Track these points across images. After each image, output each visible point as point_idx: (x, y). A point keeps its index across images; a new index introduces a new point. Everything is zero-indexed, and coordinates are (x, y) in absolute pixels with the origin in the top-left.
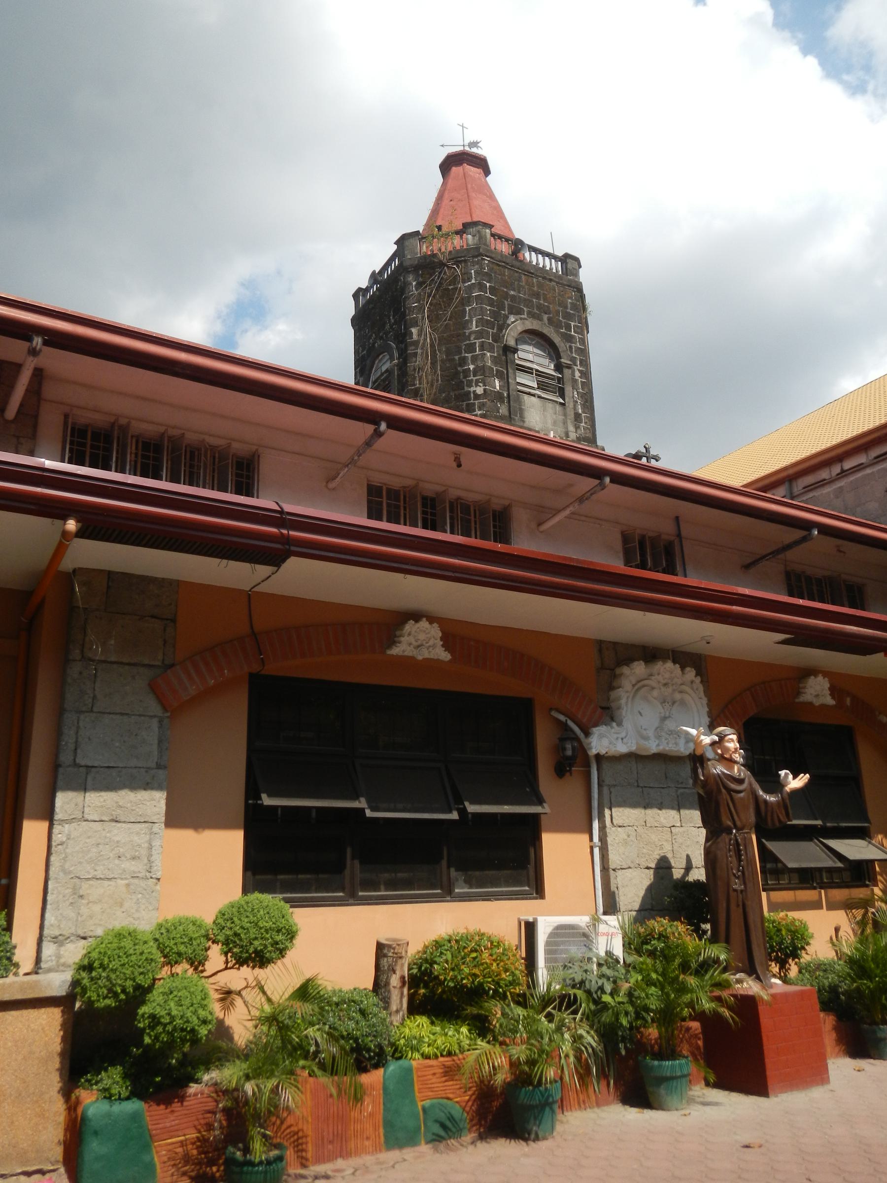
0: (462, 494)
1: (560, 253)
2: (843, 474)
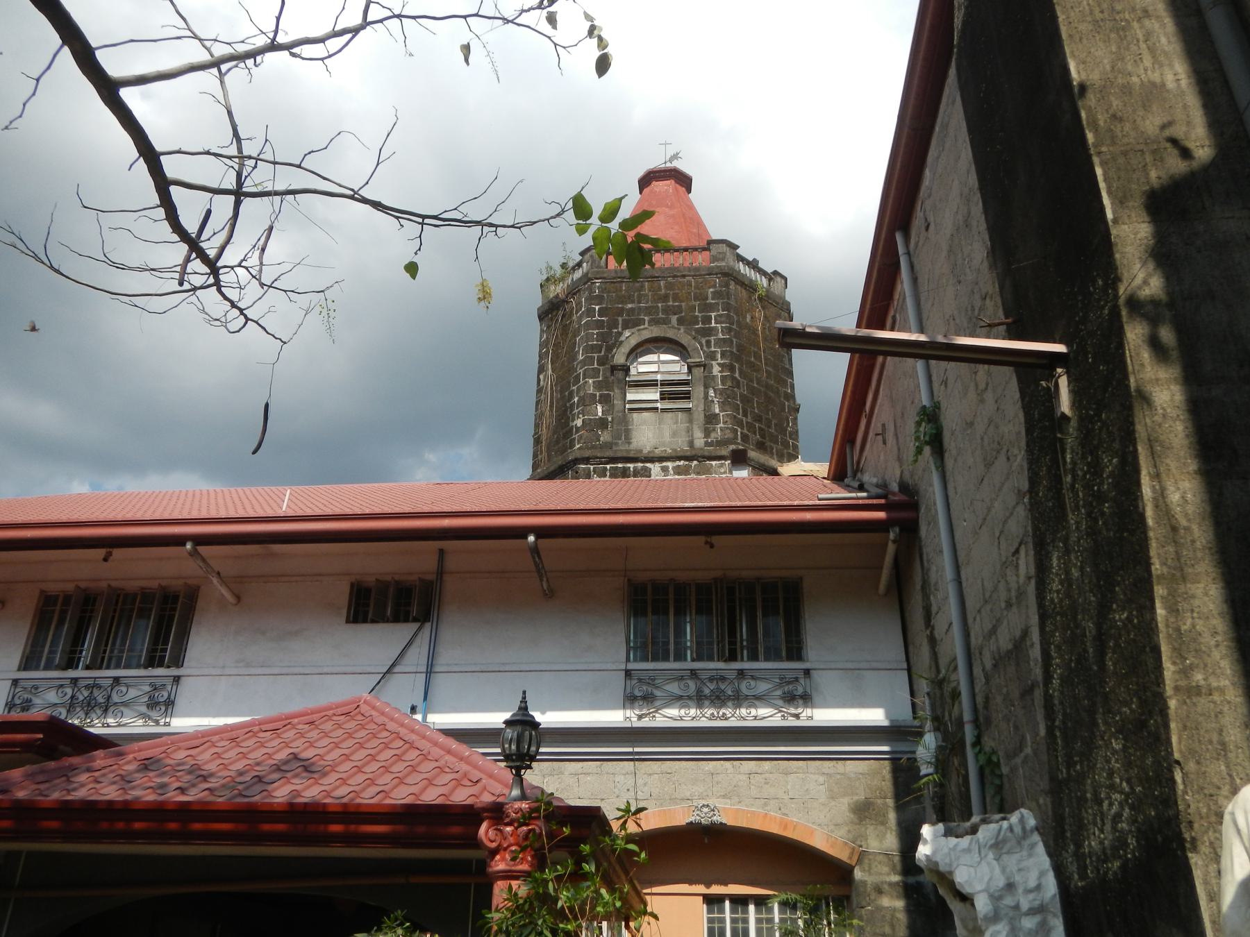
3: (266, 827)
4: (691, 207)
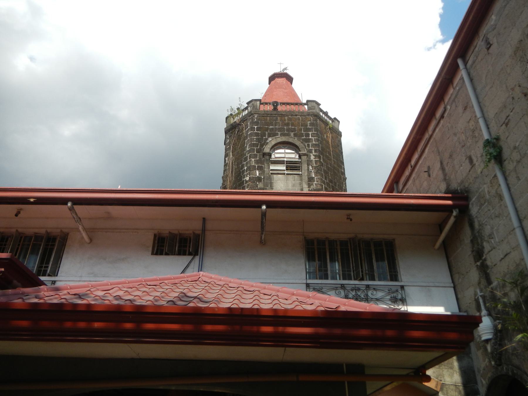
0: (36, 231)
3: (209, 328)
4: (293, 90)
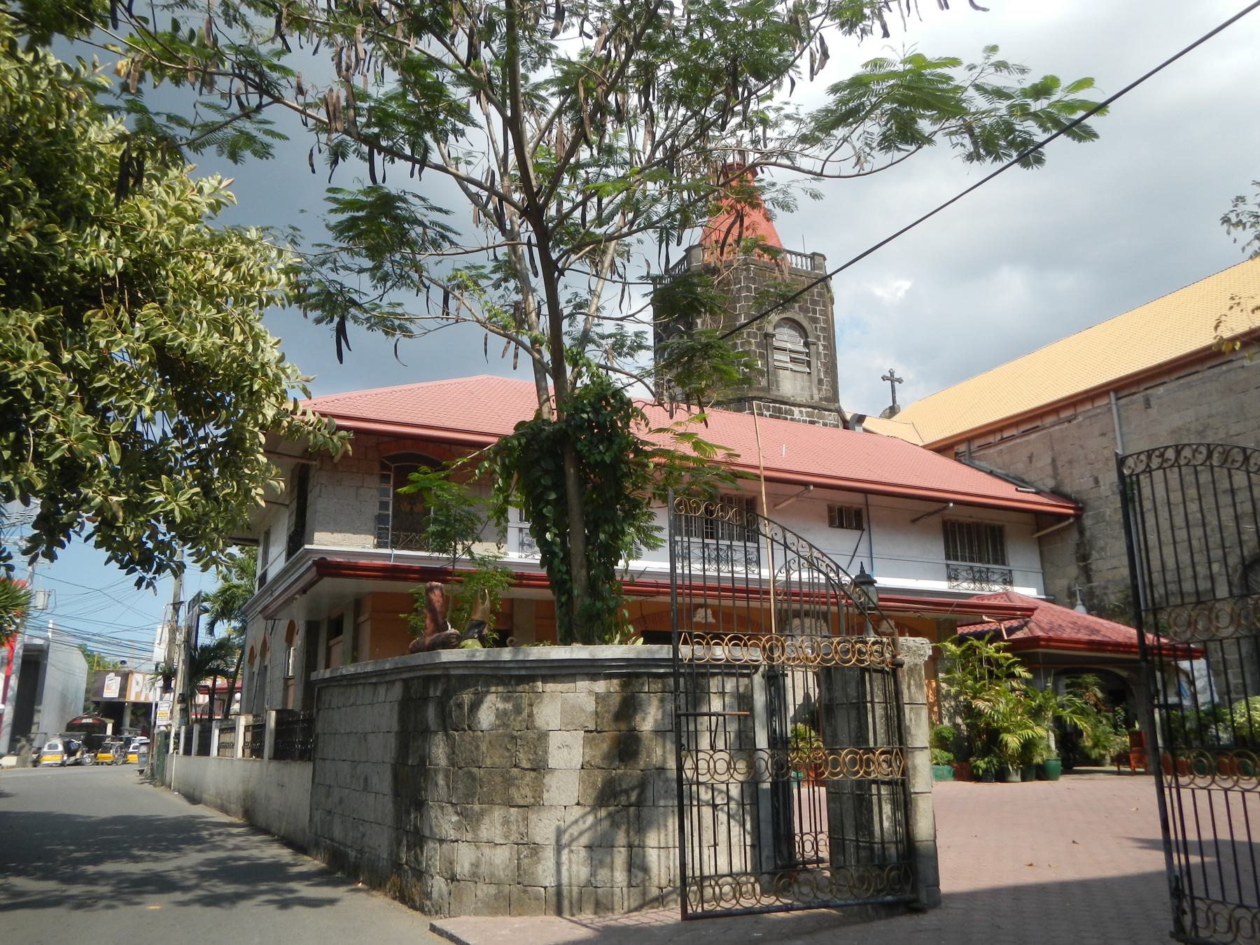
1: (808, 252)
2: (1003, 440)
